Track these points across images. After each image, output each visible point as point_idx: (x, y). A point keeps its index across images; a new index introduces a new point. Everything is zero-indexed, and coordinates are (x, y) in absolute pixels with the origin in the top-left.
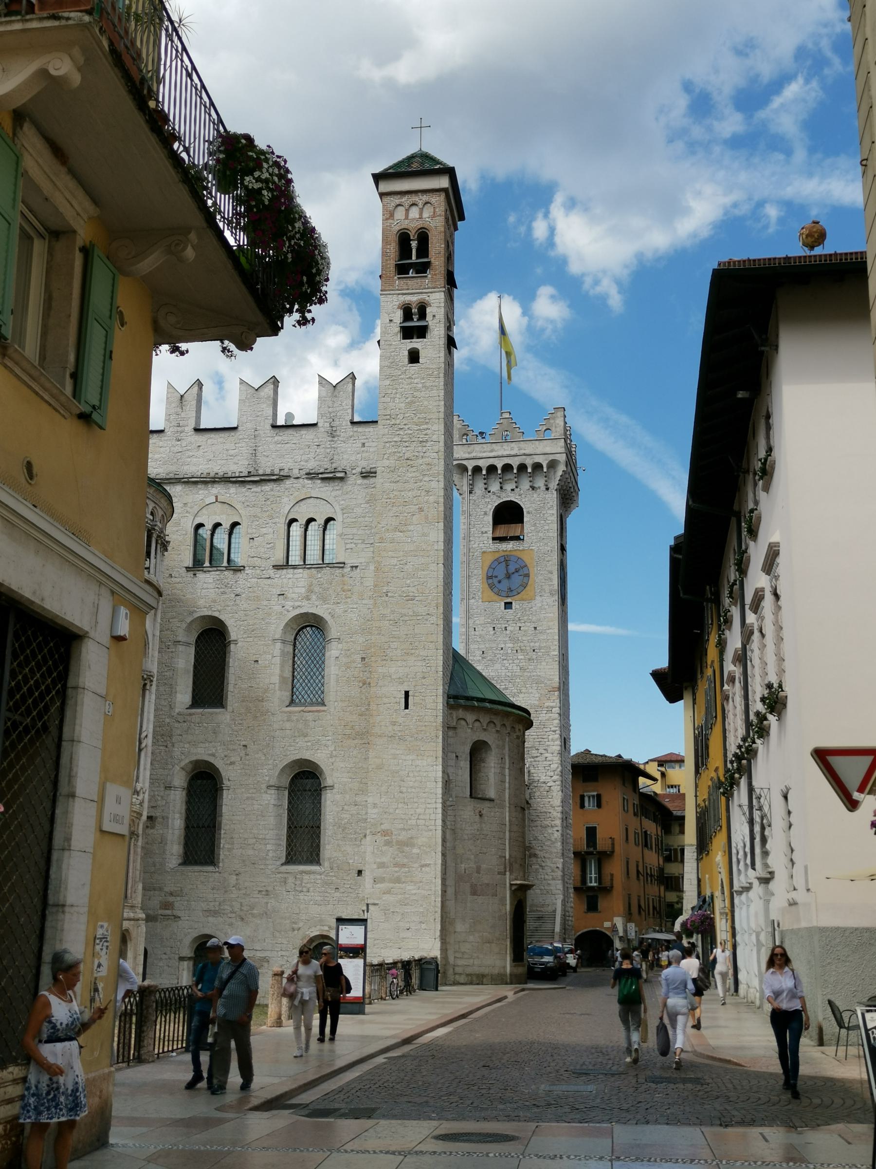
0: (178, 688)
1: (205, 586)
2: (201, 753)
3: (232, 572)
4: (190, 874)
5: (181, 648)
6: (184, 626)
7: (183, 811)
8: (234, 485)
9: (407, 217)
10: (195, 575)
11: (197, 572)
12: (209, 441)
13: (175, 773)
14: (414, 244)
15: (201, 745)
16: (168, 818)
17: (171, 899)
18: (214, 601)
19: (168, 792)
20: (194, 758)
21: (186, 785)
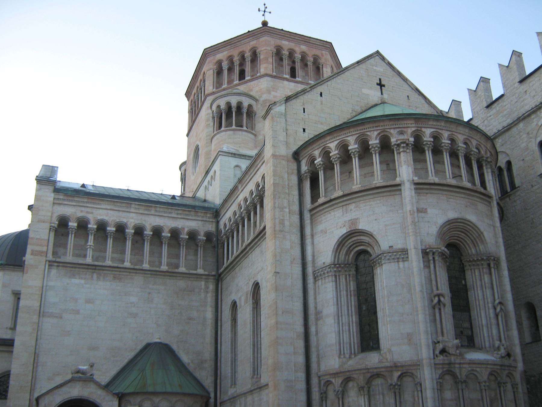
12: (531, 84)
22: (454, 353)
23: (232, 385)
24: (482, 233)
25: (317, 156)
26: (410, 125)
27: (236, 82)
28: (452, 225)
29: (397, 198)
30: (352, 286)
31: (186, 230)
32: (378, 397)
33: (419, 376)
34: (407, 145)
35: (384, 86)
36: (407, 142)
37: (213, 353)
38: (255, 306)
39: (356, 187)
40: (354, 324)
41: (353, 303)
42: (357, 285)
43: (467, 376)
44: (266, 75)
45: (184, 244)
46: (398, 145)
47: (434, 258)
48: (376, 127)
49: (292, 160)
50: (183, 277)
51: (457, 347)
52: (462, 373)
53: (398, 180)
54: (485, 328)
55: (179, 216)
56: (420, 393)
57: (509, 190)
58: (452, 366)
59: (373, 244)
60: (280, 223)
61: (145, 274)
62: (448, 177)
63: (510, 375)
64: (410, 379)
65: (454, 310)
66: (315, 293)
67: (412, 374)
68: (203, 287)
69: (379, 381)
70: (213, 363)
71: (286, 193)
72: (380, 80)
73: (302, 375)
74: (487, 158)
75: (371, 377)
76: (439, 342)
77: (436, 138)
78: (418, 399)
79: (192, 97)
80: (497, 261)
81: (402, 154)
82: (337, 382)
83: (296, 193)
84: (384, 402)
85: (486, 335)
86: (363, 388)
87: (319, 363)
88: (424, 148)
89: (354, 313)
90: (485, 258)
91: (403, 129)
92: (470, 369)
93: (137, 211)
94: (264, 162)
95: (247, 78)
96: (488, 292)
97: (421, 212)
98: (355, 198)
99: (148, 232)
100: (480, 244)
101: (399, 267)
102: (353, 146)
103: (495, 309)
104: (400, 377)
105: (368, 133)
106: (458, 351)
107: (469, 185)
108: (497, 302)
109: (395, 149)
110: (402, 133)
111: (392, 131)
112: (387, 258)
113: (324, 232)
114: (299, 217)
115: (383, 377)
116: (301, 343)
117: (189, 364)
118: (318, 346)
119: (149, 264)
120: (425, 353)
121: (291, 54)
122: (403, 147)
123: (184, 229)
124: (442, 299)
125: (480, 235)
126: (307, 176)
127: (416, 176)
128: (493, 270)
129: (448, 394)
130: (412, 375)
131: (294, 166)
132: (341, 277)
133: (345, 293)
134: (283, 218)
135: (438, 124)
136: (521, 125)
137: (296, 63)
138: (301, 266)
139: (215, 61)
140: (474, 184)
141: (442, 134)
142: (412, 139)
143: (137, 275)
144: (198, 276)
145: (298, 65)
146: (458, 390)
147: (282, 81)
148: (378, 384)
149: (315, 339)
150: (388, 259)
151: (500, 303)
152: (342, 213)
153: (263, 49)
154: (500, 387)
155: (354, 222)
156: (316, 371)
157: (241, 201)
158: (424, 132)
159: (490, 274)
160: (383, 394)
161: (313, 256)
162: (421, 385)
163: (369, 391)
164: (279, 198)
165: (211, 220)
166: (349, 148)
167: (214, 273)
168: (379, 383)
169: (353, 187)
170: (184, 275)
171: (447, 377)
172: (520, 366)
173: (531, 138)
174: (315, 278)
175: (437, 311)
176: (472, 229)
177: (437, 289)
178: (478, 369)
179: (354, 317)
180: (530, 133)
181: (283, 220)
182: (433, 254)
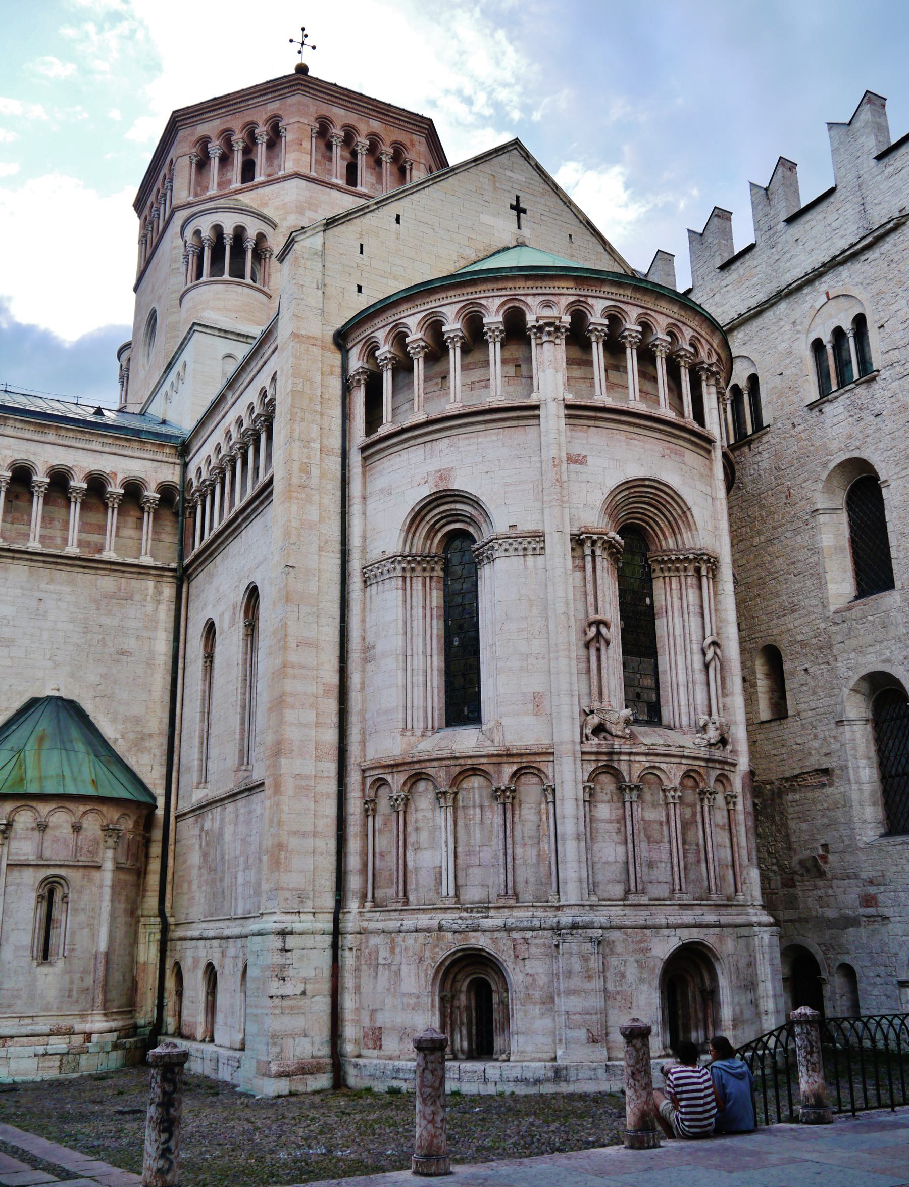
0: (828, 576)
2: (872, 663)
3: (864, 386)
4: (890, 848)
6: (820, 486)
7: (873, 754)
8: (846, 266)
10: (820, 411)
11: (822, 406)
13: (845, 698)
15: (870, 649)
16: (847, 767)
17: (872, 890)
18: (850, 436)
19: (841, 729)
20: (864, 671)
22: (619, 733)
23: (200, 783)
25: (381, 342)
26: (564, 291)
27: (237, 185)
28: (632, 490)
29: (532, 432)
30: (436, 598)
31: (120, 477)
32: (471, 812)
33: (551, 777)
34: (557, 329)
35: (524, 211)
36: (557, 323)
37: (166, 720)
38: (250, 632)
39: (452, 406)
40: (435, 673)
41: (435, 631)
42: (445, 597)
43: (641, 778)
44: (297, 175)
45: (116, 506)
46: (540, 329)
47: (593, 552)
48: (498, 289)
49: (333, 347)
50: (111, 570)
51: (627, 722)
52: (632, 770)
53: (534, 399)
54: (682, 690)
55: (107, 449)
56: (551, 806)
57: (750, 432)
58: (615, 757)
59: (480, 519)
60: (301, 470)
61: (31, 560)
62: (632, 397)
63: (722, 779)
64: (535, 780)
65: (625, 652)
66: (364, 610)
67: (539, 770)
68: (151, 591)
69: (476, 782)
70: (165, 741)
71: (316, 411)
72: (518, 198)
73: (331, 767)
74: (711, 365)
75: (460, 773)
76: (592, 712)
77: (614, 319)
78: (548, 818)
79: (146, 211)
80: (713, 563)
81: (545, 345)
82: (397, 781)
83: (337, 412)
85: (683, 702)
87: (363, 743)
88: (589, 338)
89: (435, 652)
90: (691, 557)
91: (550, 298)
92: (648, 765)
93: (19, 434)
94: (276, 348)
95: (259, 179)
96: (694, 622)
97: (575, 462)
98: (451, 428)
99: (41, 477)
100: (683, 530)
101: (525, 566)
102: (453, 326)
103: (704, 654)
104: (516, 775)
105: (483, 301)
106: (627, 731)
107: (670, 414)
108: (708, 640)
109: (532, 336)
110: (548, 305)
111: (529, 300)
112: (504, 547)
113: (387, 492)
114: (340, 460)
115: (485, 774)
116: (331, 706)
117: (116, 740)
118: (363, 712)
119: (40, 542)
122: (549, 333)
124: (604, 630)
125: (684, 513)
126: (359, 380)
127: (570, 392)
128: (704, 580)
129: (604, 811)
130: (538, 773)
131: (336, 358)
132: (414, 580)
133: (420, 611)
134: (305, 461)
135: (621, 291)
136: (783, 306)
137: (359, 156)
138: (339, 556)
139: (194, 139)
140: (681, 414)
141: (626, 312)
142: (567, 319)
143: (16, 562)
144: (142, 570)
145: (362, 161)
146: (624, 803)
147: (328, 190)
148: (473, 788)
149: (359, 698)
150: (506, 550)
151: (714, 643)
152: (423, 458)
153: (292, 121)
154: (702, 800)
155: (443, 475)
156: (359, 760)
157: (230, 425)
158: (592, 307)
159: (700, 588)
160: (482, 807)
161: (364, 538)
162: (554, 790)
163: (455, 800)
164: (303, 420)
165: (170, 460)
166: (444, 329)
167: (173, 565)
168: (476, 785)
169: (447, 407)
170: (112, 566)
171: (605, 779)
172: (743, 763)
173: (798, 332)
174: (365, 582)
175: (593, 652)
176: (671, 501)
177: (597, 612)
178: (663, 766)
179: (435, 658)
180: (798, 322)
181: (308, 464)
182: (594, 543)
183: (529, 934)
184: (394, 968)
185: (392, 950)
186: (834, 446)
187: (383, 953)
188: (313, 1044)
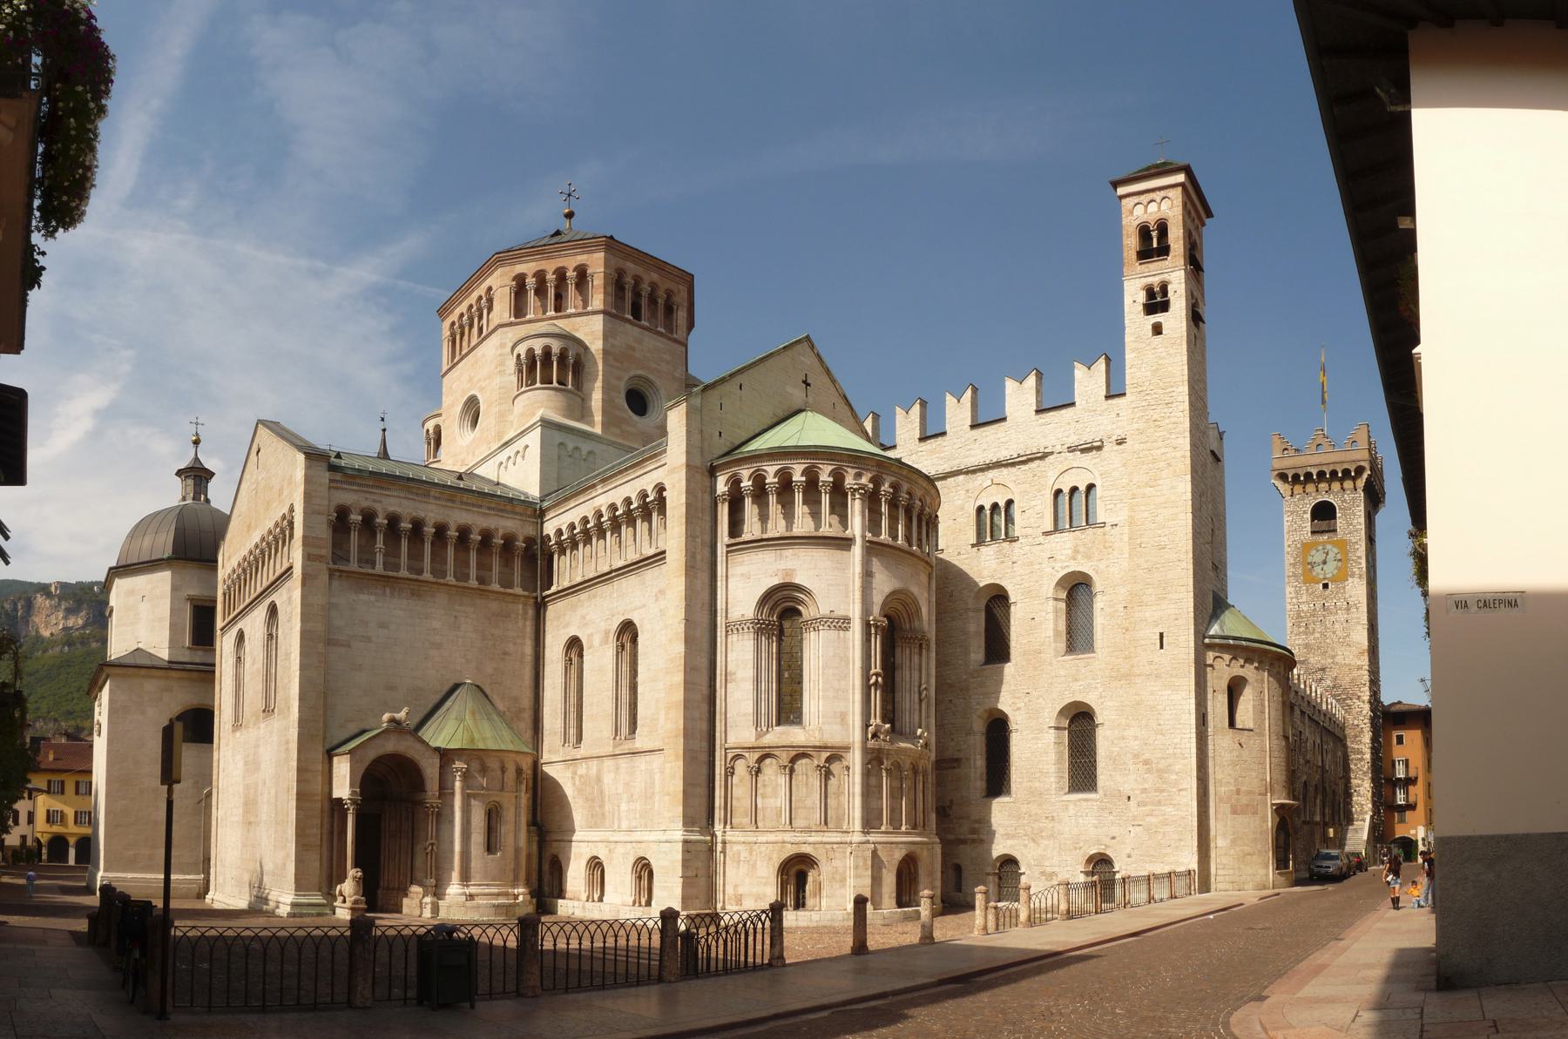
1: (988, 558)
5: (971, 614)
6: (973, 595)
9: (1146, 212)
14: (1154, 234)
21: (984, 731)
24: (920, 609)
31: (501, 532)
32: (800, 777)
84: (807, 784)
85: (907, 720)
86: (785, 767)
96: (916, 675)
101: (839, 637)
103: (920, 694)
108: (924, 687)
120: (856, 736)
121: (638, 280)
123: (498, 529)
128: (924, 650)
145: (644, 302)
147: (623, 323)
151: (926, 689)
154: (916, 776)
159: (921, 655)
180: (970, 491)
183: (835, 846)
184: (751, 863)
185: (751, 854)
186: (986, 573)
187: (744, 855)
188: (700, 902)
